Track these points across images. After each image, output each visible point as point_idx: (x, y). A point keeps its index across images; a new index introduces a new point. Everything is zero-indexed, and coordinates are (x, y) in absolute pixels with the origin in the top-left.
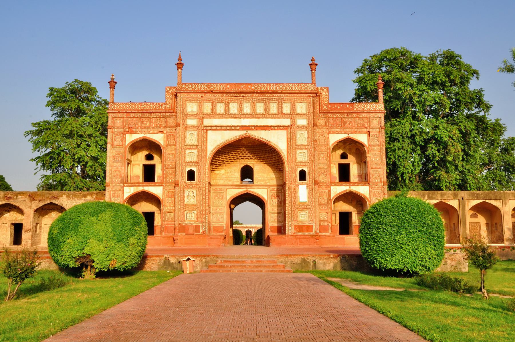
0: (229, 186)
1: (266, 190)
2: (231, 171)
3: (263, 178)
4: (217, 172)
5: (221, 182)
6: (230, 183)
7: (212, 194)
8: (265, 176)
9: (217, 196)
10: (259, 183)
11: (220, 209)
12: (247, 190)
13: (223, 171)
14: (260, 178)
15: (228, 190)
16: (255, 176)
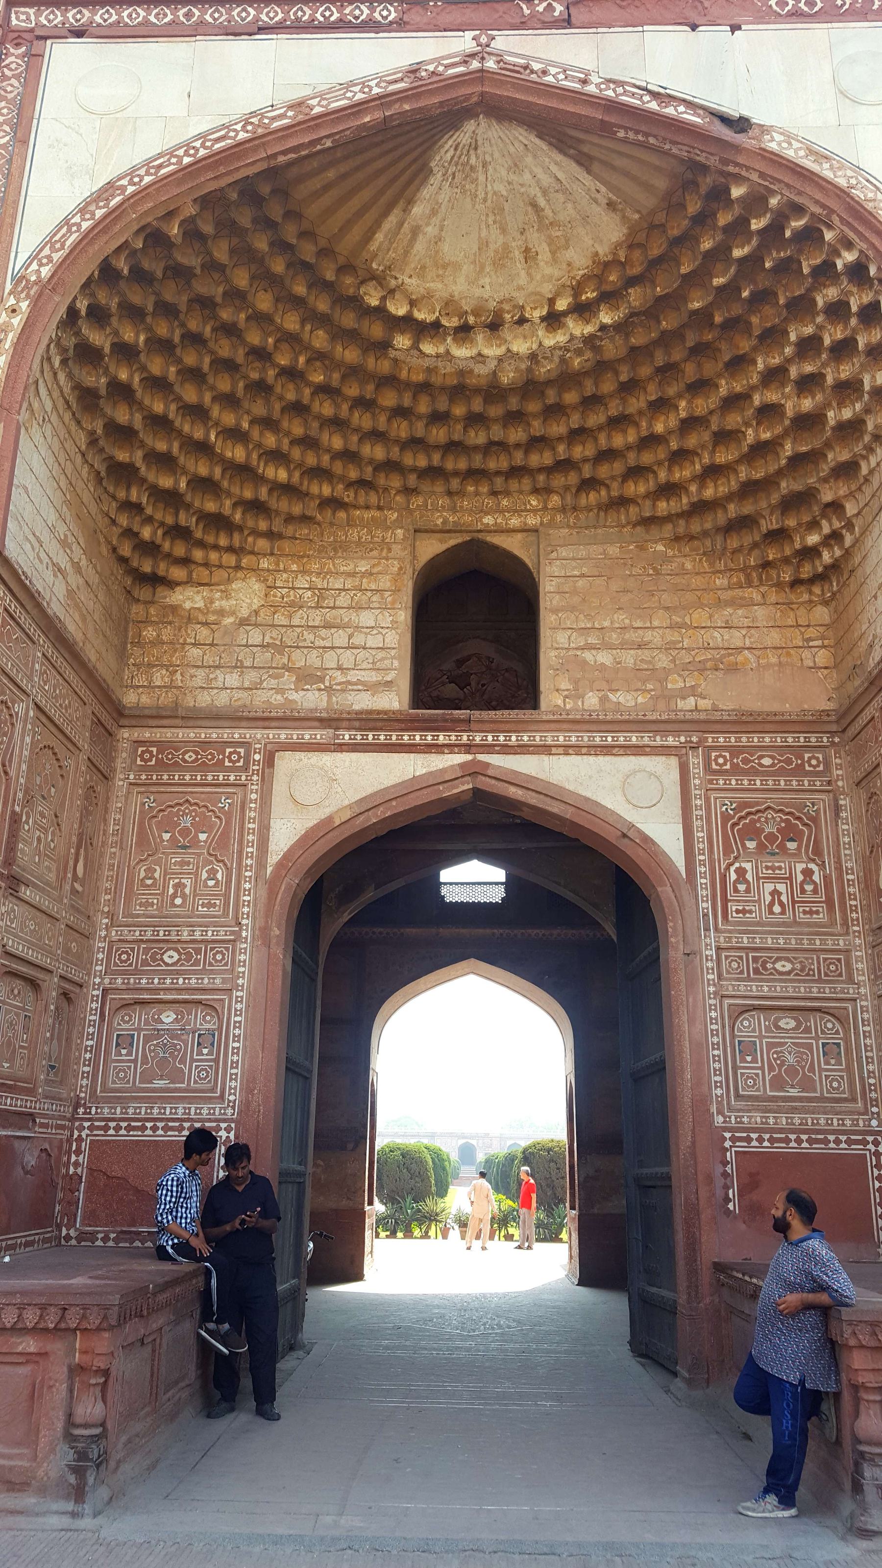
0: (291, 719)
1: (666, 769)
2: (320, 594)
3: (629, 658)
4: (189, 599)
5: (224, 689)
6: (311, 699)
7: (126, 801)
8: (654, 637)
9: (169, 825)
10: (592, 701)
11: (192, 951)
12: (473, 771)
13: (246, 595)
14: (604, 658)
15: (285, 762)
16: (558, 638)
